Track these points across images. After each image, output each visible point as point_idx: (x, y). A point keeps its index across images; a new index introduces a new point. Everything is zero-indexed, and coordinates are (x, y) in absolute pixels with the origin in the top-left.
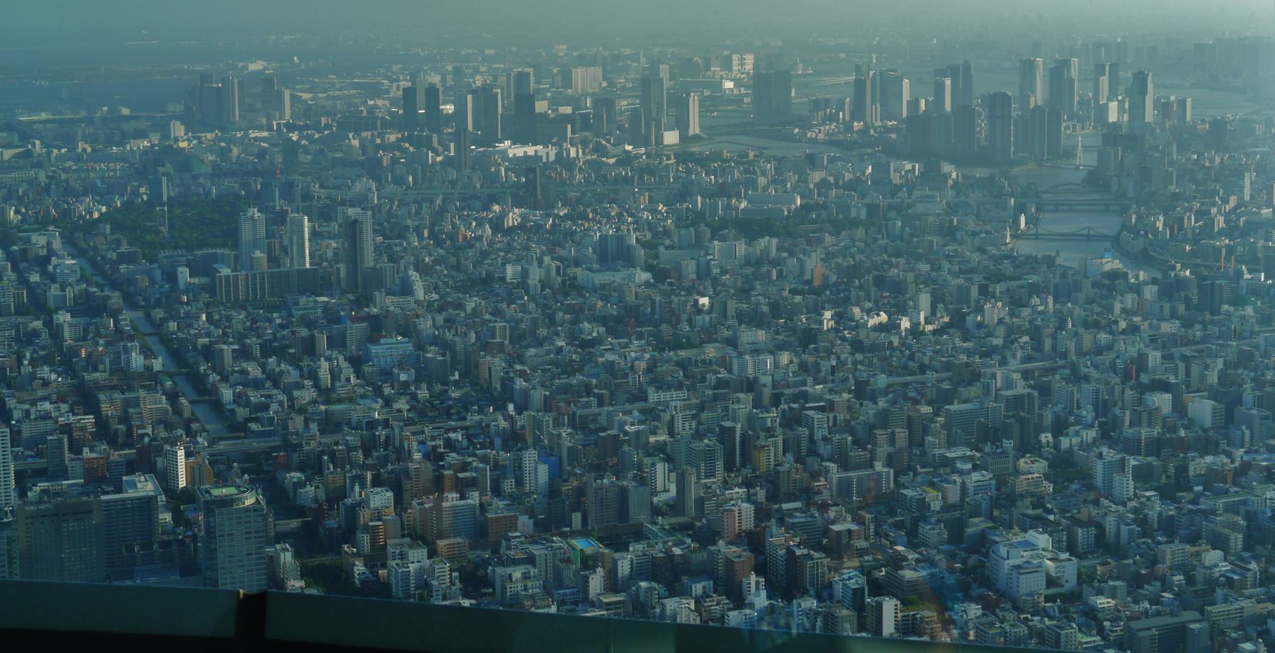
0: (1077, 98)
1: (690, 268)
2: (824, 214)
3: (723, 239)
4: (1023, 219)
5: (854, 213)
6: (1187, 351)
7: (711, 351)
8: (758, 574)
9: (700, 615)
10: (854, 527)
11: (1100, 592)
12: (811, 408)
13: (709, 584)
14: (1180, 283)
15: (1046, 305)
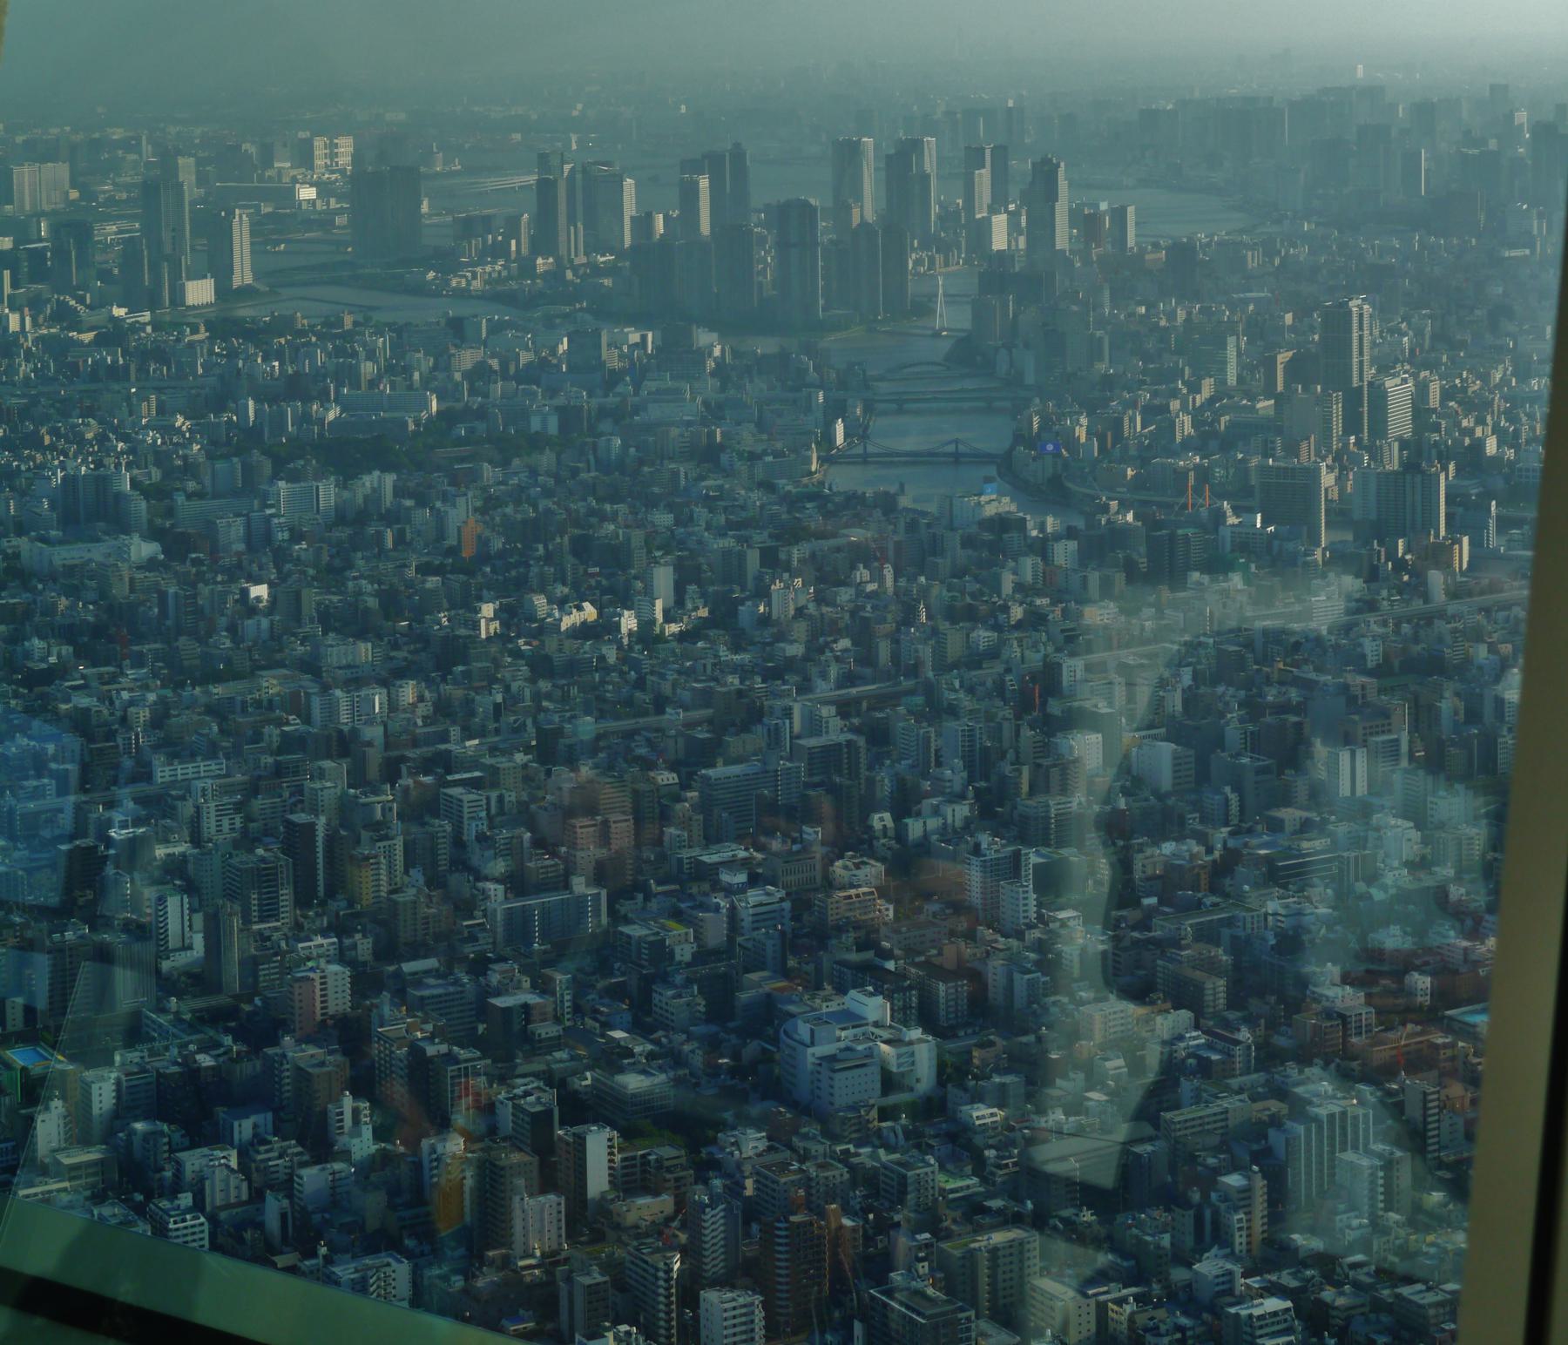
0: (935, 209)
1: (233, 531)
2: (481, 427)
3: (294, 477)
4: (840, 428)
5: (535, 424)
6: (1129, 657)
7: (271, 685)
8: (356, 1095)
9: (249, 1179)
10: (533, 999)
11: (977, 1098)
12: (456, 783)
13: (264, 1119)
14: (1119, 535)
15: (881, 580)
